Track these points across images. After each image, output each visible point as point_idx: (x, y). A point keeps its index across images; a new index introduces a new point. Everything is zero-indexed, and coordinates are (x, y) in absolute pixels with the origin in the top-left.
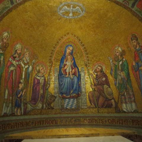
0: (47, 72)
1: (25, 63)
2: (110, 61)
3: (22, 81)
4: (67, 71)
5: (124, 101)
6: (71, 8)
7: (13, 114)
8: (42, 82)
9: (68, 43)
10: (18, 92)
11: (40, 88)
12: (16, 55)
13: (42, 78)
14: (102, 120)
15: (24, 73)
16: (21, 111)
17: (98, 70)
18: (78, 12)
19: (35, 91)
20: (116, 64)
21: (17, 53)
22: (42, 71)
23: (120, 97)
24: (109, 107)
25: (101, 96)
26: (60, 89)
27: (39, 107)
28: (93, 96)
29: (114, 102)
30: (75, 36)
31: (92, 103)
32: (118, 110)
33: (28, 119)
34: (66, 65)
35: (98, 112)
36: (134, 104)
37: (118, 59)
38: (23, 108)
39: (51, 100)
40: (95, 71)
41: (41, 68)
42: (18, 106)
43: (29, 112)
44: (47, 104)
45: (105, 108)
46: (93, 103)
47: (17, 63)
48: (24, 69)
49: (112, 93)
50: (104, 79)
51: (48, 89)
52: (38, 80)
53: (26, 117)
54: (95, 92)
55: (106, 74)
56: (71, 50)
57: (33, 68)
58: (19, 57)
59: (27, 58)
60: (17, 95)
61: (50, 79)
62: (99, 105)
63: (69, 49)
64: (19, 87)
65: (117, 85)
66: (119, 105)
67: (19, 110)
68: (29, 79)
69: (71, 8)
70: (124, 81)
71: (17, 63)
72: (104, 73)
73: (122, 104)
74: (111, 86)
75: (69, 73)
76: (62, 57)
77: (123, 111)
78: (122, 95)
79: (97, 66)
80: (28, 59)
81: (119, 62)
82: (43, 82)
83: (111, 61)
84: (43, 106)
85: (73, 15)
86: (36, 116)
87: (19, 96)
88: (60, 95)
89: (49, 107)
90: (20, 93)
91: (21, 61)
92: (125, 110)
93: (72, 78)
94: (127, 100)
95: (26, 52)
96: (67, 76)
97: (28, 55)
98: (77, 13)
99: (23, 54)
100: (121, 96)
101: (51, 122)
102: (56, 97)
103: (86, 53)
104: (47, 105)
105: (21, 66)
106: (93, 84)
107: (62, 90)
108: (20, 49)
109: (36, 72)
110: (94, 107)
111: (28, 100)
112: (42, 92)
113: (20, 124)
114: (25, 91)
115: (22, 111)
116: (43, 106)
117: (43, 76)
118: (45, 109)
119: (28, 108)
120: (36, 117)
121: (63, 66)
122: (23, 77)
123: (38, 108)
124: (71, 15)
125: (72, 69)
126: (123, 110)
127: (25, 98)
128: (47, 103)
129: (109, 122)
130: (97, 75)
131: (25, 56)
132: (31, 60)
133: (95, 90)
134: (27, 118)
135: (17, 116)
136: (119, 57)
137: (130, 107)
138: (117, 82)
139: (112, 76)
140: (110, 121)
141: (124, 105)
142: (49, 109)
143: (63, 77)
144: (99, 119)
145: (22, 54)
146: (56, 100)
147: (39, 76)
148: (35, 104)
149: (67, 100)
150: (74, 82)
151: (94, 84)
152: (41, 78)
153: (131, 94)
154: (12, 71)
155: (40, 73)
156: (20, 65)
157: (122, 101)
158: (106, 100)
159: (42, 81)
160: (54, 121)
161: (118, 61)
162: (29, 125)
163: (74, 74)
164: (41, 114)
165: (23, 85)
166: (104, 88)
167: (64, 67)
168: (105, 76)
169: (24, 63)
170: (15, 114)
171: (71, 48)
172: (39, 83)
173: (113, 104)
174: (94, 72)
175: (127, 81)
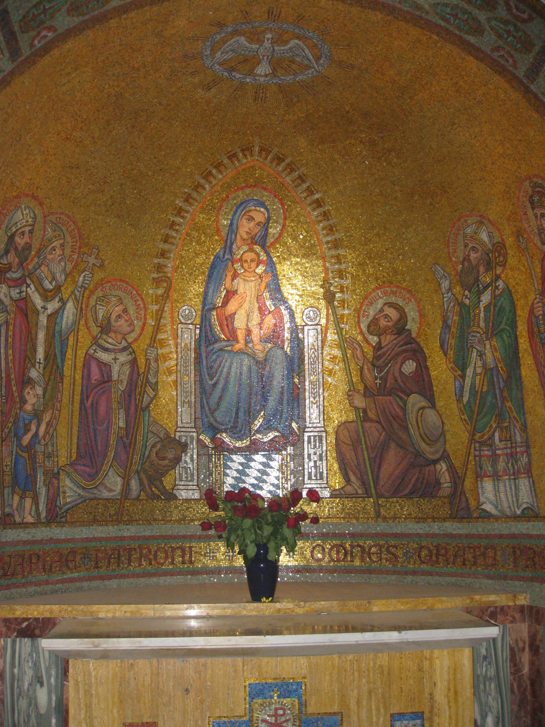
0: (143, 329)
1: (46, 291)
2: (440, 285)
3: (34, 374)
4: (239, 323)
5: (488, 468)
6: (267, 44)
8: (122, 377)
9: (248, 191)
10: (21, 424)
11: (115, 406)
13: (123, 358)
14: (393, 550)
15: (41, 336)
16: (37, 504)
17: (383, 323)
18: (298, 59)
20: (467, 301)
21: (16, 249)
22: (122, 322)
23: (472, 450)
24: (423, 496)
25: (393, 445)
26: (202, 407)
27: (111, 491)
28: (355, 444)
29: (447, 474)
30: (279, 159)
31: (353, 478)
33: (67, 541)
34: (235, 292)
35: (378, 515)
36: (526, 481)
37: (477, 280)
38: (43, 492)
39: (164, 459)
40: (369, 327)
41: (118, 309)
43: (66, 511)
44: (143, 476)
45: (405, 496)
46: (355, 474)
47: (15, 293)
48: (43, 320)
49: (443, 434)
50: (410, 367)
51: (148, 406)
54: (367, 425)
55: (422, 344)
56: (258, 224)
57: (81, 311)
58: (21, 264)
61: (156, 361)
62: (382, 483)
63: (251, 219)
64: (24, 401)
65: (465, 399)
66: (468, 484)
67: (28, 502)
68: (63, 361)
69: (267, 44)
70: (493, 381)
72: (410, 340)
73: (481, 481)
74: (440, 404)
75: (249, 332)
76: (217, 257)
77: (484, 510)
78: (482, 444)
79: (380, 304)
80: (57, 269)
81: (480, 293)
82: (125, 378)
83: (445, 284)
84: (126, 486)
85: (274, 69)
86: (100, 528)
87: (26, 439)
89: (157, 492)
90: (29, 430)
91: (29, 282)
92: (488, 507)
93: (261, 356)
94: (501, 465)
95: (50, 241)
96: (238, 346)
97: (58, 252)
98: (293, 62)
99: (39, 249)
100: (477, 445)
101: (166, 557)
102: (184, 447)
103: (329, 239)
104: (145, 481)
105: (29, 305)
106: (361, 388)
107: (212, 413)
108: (27, 229)
109: (95, 330)
110: (360, 491)
111: (63, 460)
113: (34, 561)
114: (47, 417)
115: (41, 508)
116: (128, 484)
117: (124, 349)
118: (137, 499)
119: (64, 492)
120: (98, 531)
123: (106, 494)
124: (263, 69)
126: (483, 507)
127: (50, 449)
128: (145, 471)
129: (419, 556)
130: (378, 347)
131: (45, 257)
133: (366, 418)
134: (63, 537)
135: (24, 525)
136: (482, 269)
137: (509, 494)
138: (467, 388)
139: (445, 354)
140: (424, 553)
141: (488, 485)
143: (221, 350)
144: (381, 547)
145: (36, 246)
147: (106, 350)
148: (92, 477)
149: (238, 459)
150: (271, 376)
151: (366, 387)
152: (115, 359)
153: (519, 439)
155: (112, 335)
156: (26, 301)
157: (481, 468)
160: (179, 552)
161: (474, 289)
162: (71, 565)
164: (117, 519)
165: (39, 391)
166: (409, 405)
167: (226, 303)
169: (41, 291)
170: (13, 516)
171: (259, 216)
172: (109, 380)
173: (442, 481)
174: (364, 329)
175: (505, 382)
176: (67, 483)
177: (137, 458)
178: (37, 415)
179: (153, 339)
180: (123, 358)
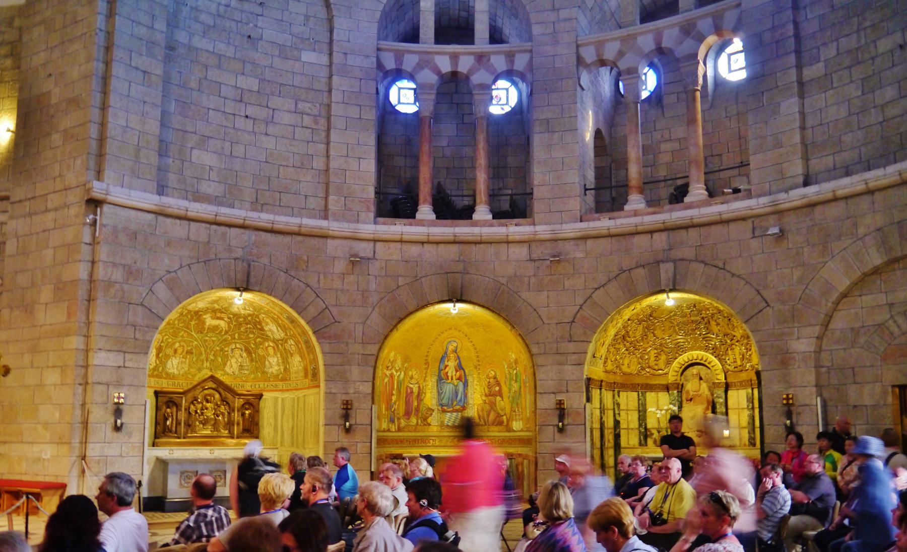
4: (449, 374)
13: (417, 386)
15: (396, 382)
19: (408, 403)
28: (483, 410)
32: (509, 429)
50: (497, 388)
52: (411, 389)
57: (405, 374)
59: (398, 364)
72: (497, 381)
88: (440, 408)
93: (456, 384)
111: (401, 415)
112: (415, 404)
121: (443, 368)
125: (457, 371)
130: (489, 382)
132: (403, 365)
142: (425, 425)
148: (408, 419)
149: (449, 414)
158: (497, 417)
159: (415, 390)
163: (459, 379)
164: (415, 431)
167: (445, 368)
168: (499, 384)
176: (402, 421)
178: (395, 403)
179: (425, 380)
180: (417, 386)
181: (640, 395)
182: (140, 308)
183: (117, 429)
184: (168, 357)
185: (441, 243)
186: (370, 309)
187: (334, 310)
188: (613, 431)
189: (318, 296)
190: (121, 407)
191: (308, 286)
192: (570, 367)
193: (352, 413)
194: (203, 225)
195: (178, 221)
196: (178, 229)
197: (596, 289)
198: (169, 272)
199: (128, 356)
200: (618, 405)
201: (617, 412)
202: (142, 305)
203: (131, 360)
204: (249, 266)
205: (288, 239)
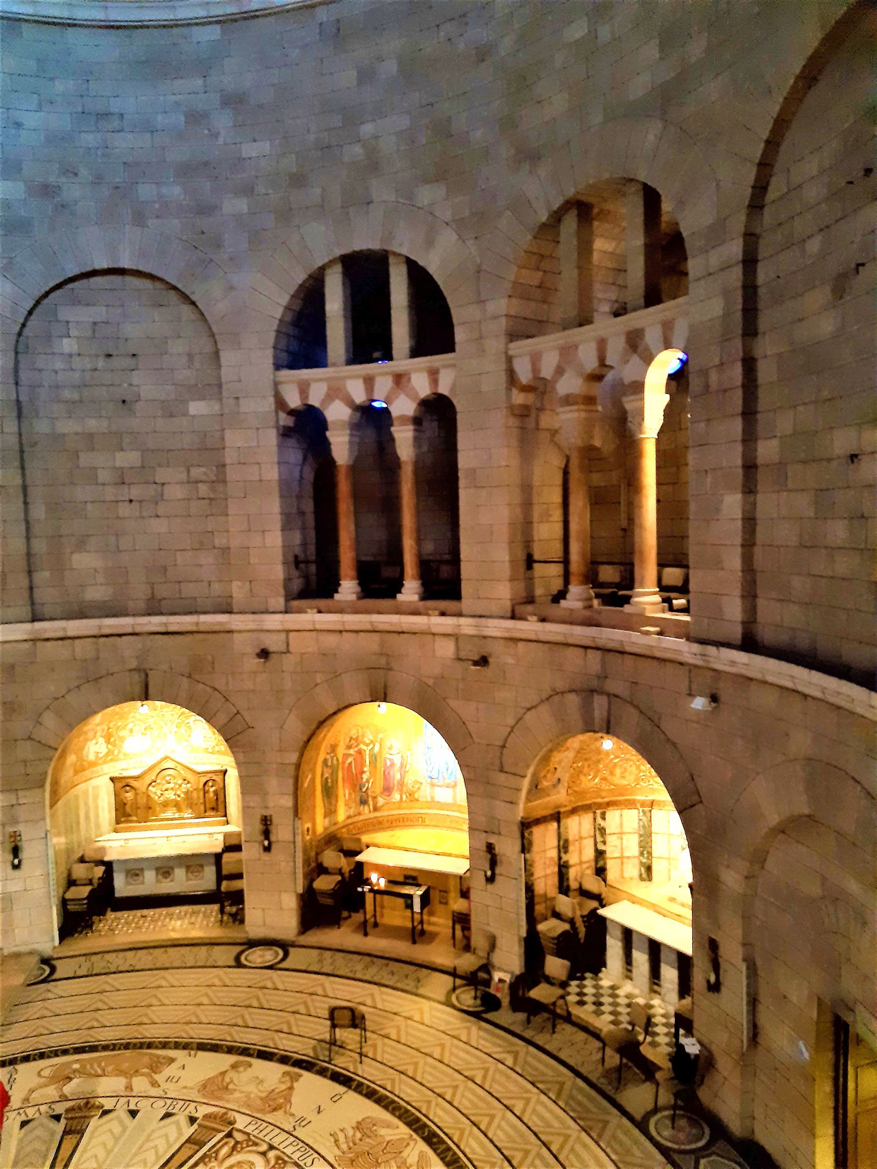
3: (365, 769)
7: (359, 814)
12: (352, 742)
15: (367, 757)
42: (364, 802)
48: (368, 752)
53: (377, 814)
60: (361, 789)
71: (356, 749)
84: (401, 797)
87: (364, 790)
114: (371, 781)
122: (368, 762)
146: (423, 787)
154: (350, 763)
164: (399, 808)
177: (405, 789)
178: (368, 781)
181: (641, 814)
182: (29, 743)
183: (16, 867)
184: (122, 739)
185: (361, 631)
186: (287, 712)
187: (246, 714)
188: (593, 864)
189: (227, 700)
190: (19, 844)
191: (215, 689)
192: (503, 804)
193: (273, 829)
194: (90, 640)
195: (60, 642)
196: (61, 651)
197: (529, 709)
198: (57, 699)
199: (20, 793)
200: (602, 831)
201: (599, 839)
202: (30, 738)
203: (25, 796)
204: (147, 675)
205: (189, 638)
